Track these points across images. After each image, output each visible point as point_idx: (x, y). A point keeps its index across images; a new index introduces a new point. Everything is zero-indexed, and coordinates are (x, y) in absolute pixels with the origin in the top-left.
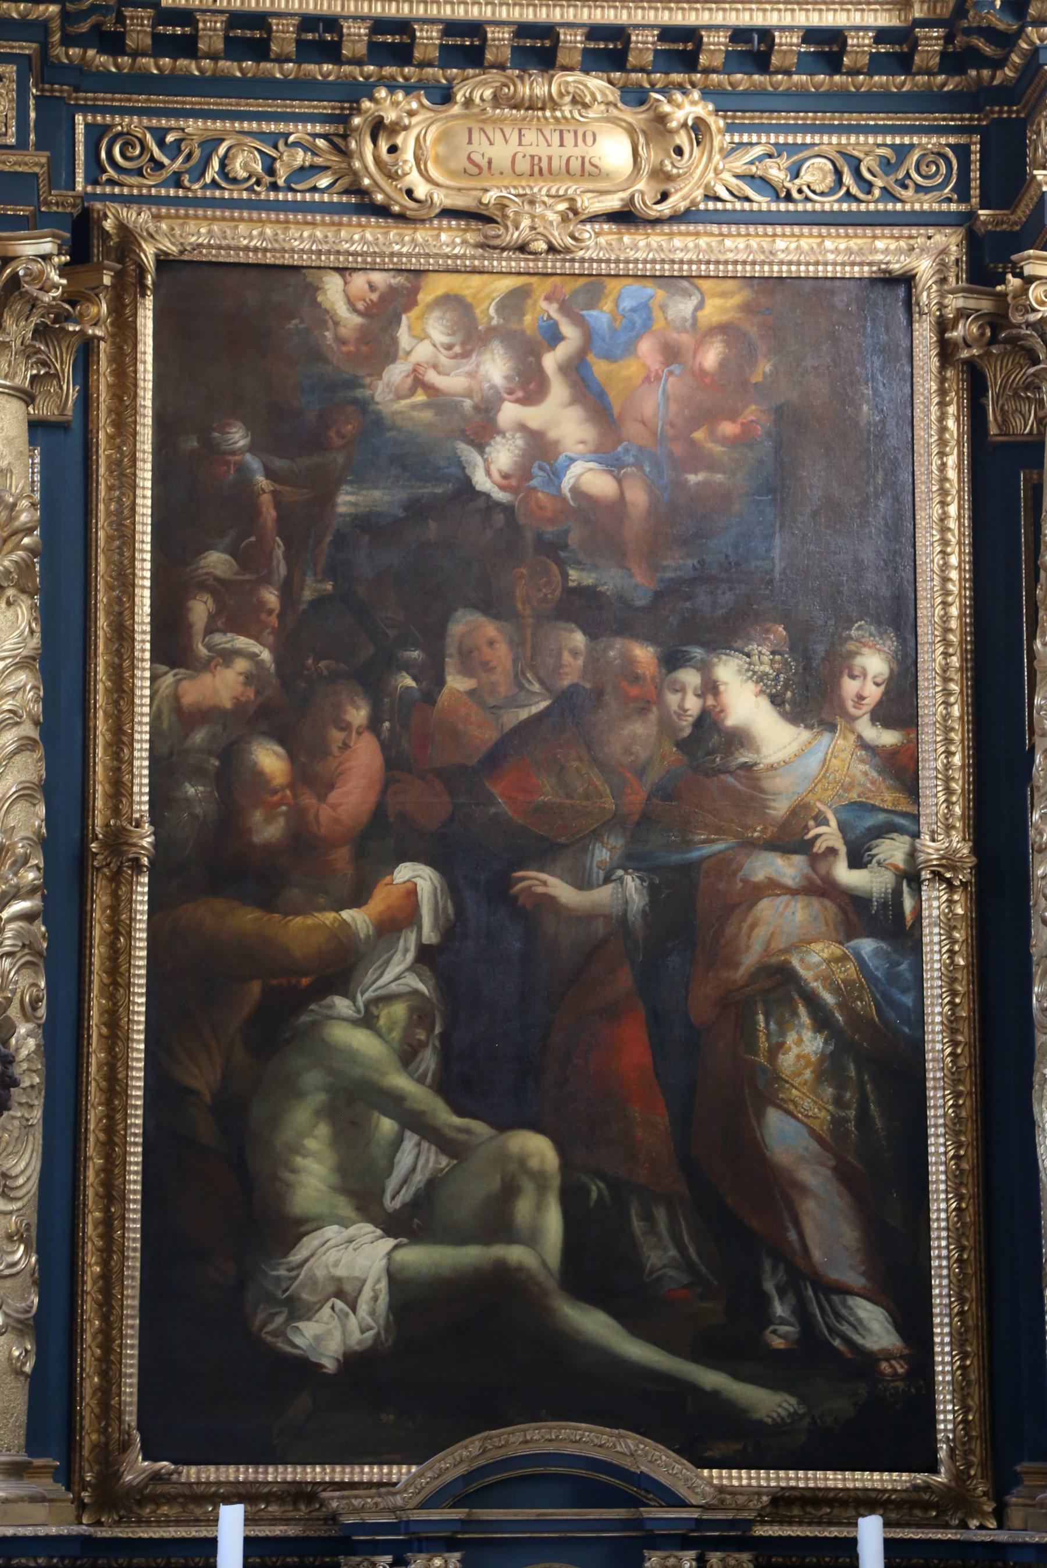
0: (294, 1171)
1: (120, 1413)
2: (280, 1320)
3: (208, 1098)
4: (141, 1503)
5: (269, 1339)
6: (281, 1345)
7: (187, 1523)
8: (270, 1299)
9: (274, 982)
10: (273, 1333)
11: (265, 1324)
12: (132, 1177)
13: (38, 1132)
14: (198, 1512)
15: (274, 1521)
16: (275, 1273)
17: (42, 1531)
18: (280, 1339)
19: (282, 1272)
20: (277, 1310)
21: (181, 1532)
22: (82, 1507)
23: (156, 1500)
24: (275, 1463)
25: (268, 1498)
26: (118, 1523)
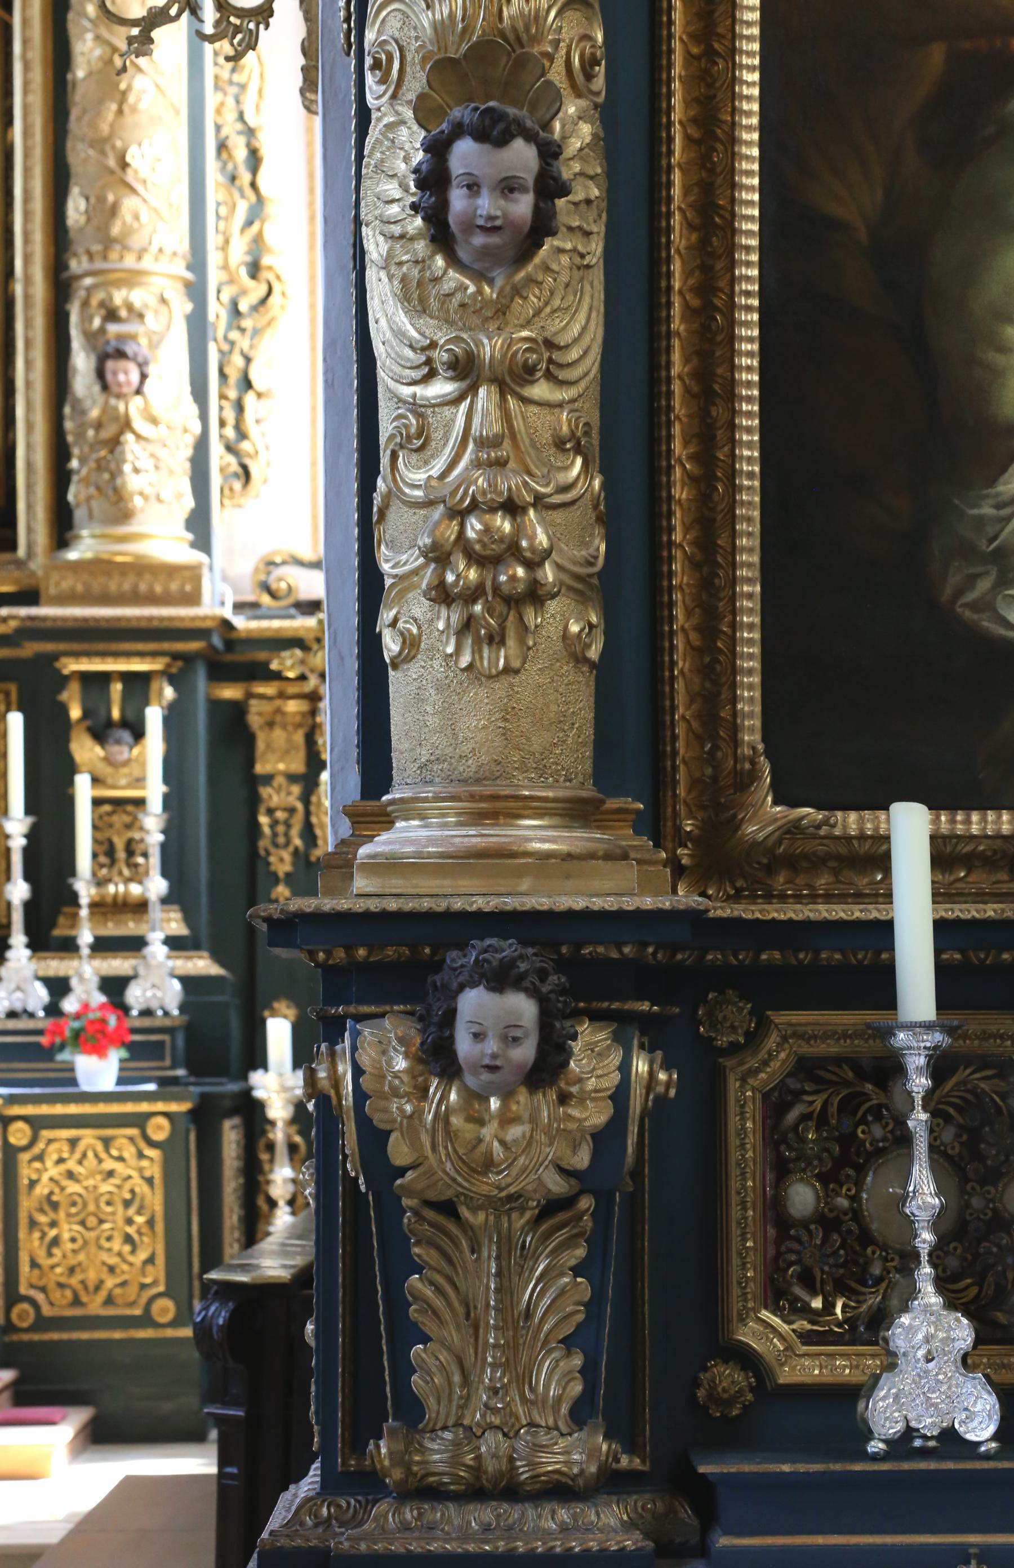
0: (1002, 349)
1: (735, 730)
2: (984, 585)
3: (862, 233)
4: (770, 869)
5: (968, 614)
6: (987, 624)
7: (843, 898)
8: (969, 552)
9: (967, 45)
10: (973, 606)
11: (959, 593)
12: (745, 361)
13: (598, 276)
14: (862, 882)
15: (981, 897)
16: (975, 512)
17: (630, 904)
18: (985, 616)
19: (987, 510)
20: (979, 569)
21: (838, 912)
22: (679, 871)
23: (792, 863)
24: (983, 807)
25: (970, 861)
26: (737, 897)
